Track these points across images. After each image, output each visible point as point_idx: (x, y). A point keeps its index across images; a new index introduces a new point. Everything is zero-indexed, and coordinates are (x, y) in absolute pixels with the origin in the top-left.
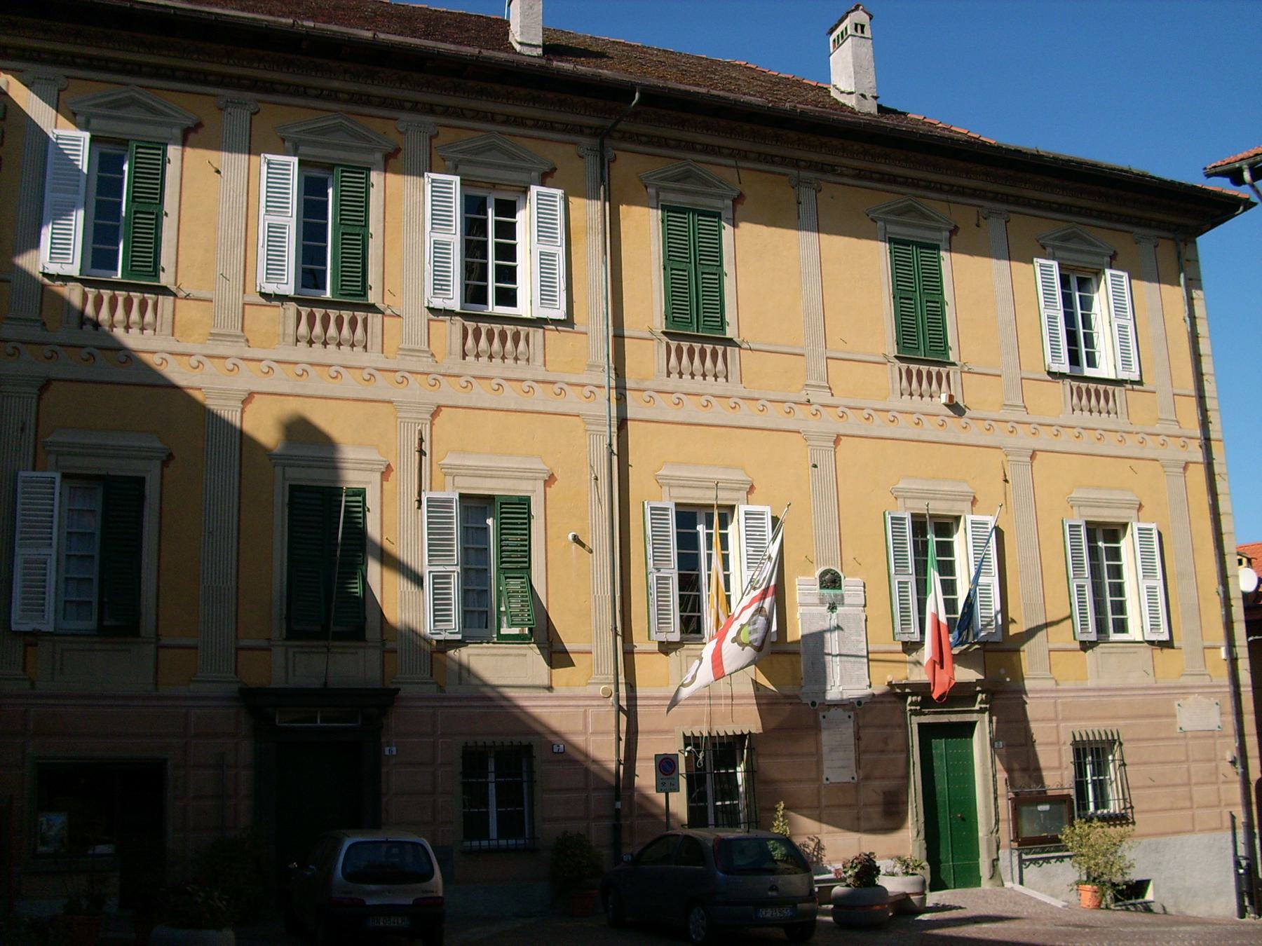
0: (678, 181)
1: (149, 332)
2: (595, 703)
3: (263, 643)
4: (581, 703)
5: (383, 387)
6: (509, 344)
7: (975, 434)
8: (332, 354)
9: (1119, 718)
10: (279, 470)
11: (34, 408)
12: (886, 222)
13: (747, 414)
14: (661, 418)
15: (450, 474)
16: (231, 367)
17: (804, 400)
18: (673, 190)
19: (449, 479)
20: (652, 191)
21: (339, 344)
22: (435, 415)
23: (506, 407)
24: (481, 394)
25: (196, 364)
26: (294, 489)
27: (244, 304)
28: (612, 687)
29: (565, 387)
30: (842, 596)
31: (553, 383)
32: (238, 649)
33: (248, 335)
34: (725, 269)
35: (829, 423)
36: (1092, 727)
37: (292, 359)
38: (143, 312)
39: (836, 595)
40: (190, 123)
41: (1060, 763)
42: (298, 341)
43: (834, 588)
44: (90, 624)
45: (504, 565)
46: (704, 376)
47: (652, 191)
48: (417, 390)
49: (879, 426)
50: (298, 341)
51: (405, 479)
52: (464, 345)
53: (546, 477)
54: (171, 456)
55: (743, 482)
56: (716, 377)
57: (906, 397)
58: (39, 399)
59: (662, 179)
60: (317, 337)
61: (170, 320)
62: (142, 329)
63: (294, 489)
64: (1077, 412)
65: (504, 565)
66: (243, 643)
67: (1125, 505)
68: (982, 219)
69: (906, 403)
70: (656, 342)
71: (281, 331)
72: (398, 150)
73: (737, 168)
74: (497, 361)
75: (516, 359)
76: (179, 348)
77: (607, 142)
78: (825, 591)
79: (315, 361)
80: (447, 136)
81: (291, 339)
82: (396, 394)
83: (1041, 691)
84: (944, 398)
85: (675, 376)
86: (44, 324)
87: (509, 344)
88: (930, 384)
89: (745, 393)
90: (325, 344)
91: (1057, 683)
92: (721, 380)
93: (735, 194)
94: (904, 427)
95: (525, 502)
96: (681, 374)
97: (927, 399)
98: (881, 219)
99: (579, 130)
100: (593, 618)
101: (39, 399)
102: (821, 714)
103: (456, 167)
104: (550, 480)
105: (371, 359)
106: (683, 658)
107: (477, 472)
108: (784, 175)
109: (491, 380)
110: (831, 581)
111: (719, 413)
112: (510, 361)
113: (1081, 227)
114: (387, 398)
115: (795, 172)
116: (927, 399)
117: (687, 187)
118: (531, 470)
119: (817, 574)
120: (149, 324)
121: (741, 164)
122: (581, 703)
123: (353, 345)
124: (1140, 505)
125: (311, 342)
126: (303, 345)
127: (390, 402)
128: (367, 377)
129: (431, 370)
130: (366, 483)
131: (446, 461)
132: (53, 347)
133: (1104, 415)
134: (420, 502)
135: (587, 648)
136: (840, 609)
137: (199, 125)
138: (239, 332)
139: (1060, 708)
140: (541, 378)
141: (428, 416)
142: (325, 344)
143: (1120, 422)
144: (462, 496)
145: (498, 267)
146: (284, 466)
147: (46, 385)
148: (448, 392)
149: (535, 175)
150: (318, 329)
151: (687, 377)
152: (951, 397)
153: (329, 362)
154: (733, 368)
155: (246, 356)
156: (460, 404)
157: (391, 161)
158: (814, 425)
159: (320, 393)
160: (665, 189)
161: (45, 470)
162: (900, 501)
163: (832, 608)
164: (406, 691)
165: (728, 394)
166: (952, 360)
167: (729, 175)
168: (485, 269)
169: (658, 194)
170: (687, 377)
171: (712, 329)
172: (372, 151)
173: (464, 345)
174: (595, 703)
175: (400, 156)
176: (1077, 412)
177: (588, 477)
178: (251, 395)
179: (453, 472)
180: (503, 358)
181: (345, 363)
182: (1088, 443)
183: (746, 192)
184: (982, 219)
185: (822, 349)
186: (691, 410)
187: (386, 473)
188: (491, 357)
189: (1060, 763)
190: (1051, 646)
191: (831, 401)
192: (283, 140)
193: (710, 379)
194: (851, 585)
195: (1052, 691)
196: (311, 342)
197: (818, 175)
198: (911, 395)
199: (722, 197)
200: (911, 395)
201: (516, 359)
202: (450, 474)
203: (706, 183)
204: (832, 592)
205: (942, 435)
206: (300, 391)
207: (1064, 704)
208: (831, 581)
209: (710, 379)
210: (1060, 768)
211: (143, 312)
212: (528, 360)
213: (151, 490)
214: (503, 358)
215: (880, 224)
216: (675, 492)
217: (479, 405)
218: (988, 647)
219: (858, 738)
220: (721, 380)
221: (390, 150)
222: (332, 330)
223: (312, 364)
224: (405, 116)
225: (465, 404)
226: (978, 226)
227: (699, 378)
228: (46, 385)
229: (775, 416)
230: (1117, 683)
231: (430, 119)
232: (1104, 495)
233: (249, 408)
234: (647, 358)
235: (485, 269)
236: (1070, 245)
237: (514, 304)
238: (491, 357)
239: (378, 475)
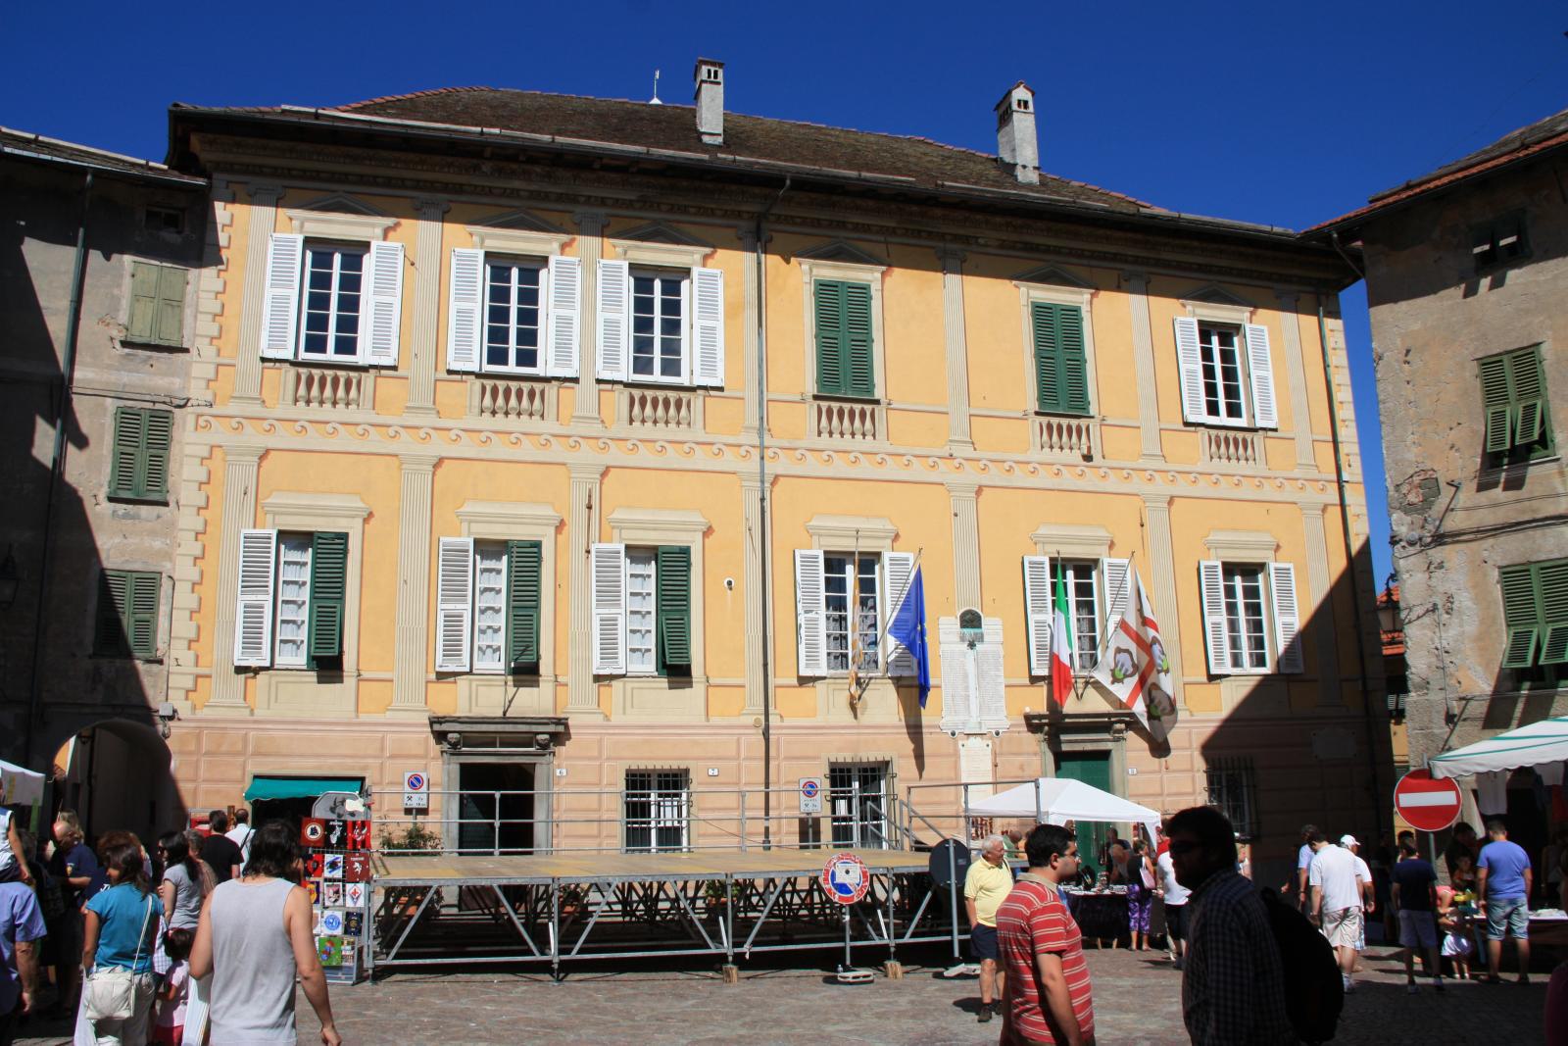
1: (353, 407)
5: (558, 451)
6: (672, 410)
7: (1113, 483)
13: (892, 469)
15: (618, 527)
17: (947, 455)
19: (616, 532)
21: (519, 414)
22: (604, 475)
24: (645, 456)
27: (436, 381)
30: (982, 635)
31: (712, 444)
33: (438, 408)
35: (972, 476)
39: (976, 634)
42: (482, 411)
46: (853, 434)
49: (1020, 478)
50: (482, 411)
52: (631, 411)
53: (704, 528)
54: (371, 515)
56: (864, 435)
57: (1047, 450)
58: (259, 466)
62: (348, 404)
70: (807, 406)
71: (468, 404)
74: (661, 425)
75: (678, 423)
78: (966, 630)
81: (477, 410)
82: (569, 457)
85: (825, 435)
86: (264, 402)
87: (672, 410)
89: (891, 449)
90: (507, 413)
92: (869, 438)
94: (1045, 479)
95: (685, 552)
96: (831, 434)
101: (259, 466)
102: (960, 743)
103: (625, 253)
104: (708, 532)
105: (549, 426)
109: (656, 442)
110: (971, 620)
111: (866, 468)
123: (531, 415)
125: (494, 413)
126: (487, 415)
127: (564, 464)
133: (1243, 462)
134: (588, 552)
136: (979, 646)
138: (431, 405)
141: (598, 476)
142: (507, 413)
146: (470, 522)
148: (616, 455)
150: (500, 400)
151: (836, 436)
155: (437, 426)
163: (972, 645)
165: (875, 450)
166: (1092, 413)
170: (836, 436)
171: (861, 391)
173: (631, 411)
179: (620, 525)
182: (1225, 489)
186: (840, 467)
187: (560, 527)
188: (655, 422)
193: (859, 437)
194: (990, 625)
196: (494, 413)
200: (1051, 447)
201: (678, 423)
202: (618, 527)
205: (1081, 484)
208: (971, 620)
209: (859, 437)
212: (689, 424)
213: (354, 544)
214: (667, 423)
220: (869, 438)
222: (513, 401)
224: (579, 209)
227: (848, 437)
229: (919, 471)
231: (602, 211)
232: (1243, 537)
233: (439, 472)
238: (655, 422)
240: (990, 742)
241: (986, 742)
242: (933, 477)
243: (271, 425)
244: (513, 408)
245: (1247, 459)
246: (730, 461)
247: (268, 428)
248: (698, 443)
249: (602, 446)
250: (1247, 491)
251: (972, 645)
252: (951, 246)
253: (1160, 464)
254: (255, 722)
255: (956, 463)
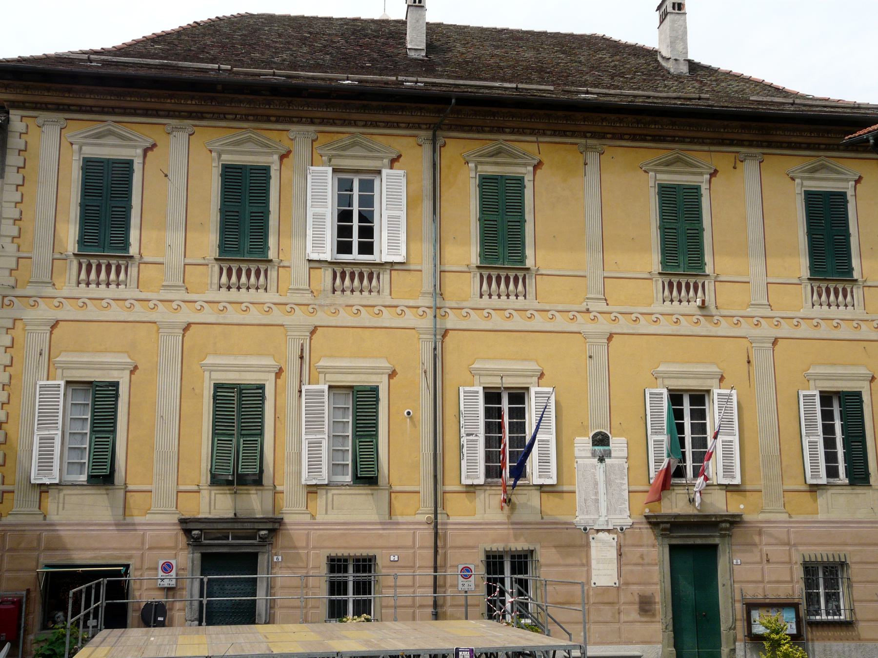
0: (492, 156)
1: (122, 287)
2: (422, 527)
3: (195, 488)
4: (411, 527)
5: (277, 316)
6: (366, 282)
7: (724, 328)
8: (243, 295)
9: (847, 544)
10: (207, 374)
11: (48, 339)
12: (656, 172)
13: (539, 322)
14: (475, 328)
15: (322, 372)
16: (176, 307)
17: (584, 309)
18: (488, 163)
19: (322, 376)
20: (472, 165)
21: (248, 288)
22: (313, 332)
23: (362, 325)
24: (345, 318)
25: (129, 306)
26: (218, 387)
27: (185, 265)
28: (432, 516)
29: (448, 310)
30: (610, 451)
31: (397, 307)
32: (178, 492)
33: (188, 286)
34: (527, 217)
35: (604, 326)
36: (822, 552)
37: (217, 299)
38: (118, 274)
39: (605, 451)
40: (148, 145)
41: (792, 577)
42: (220, 287)
43: (604, 445)
44: (84, 478)
45: (243, 432)
46: (508, 296)
47: (472, 165)
48: (300, 317)
49: (644, 326)
50: (220, 287)
51: (291, 378)
52: (334, 284)
53: (390, 372)
54: (136, 368)
55: (534, 371)
56: (517, 296)
57: (668, 303)
58: (51, 333)
59: (480, 156)
60: (233, 284)
61: (136, 278)
62: (118, 285)
63: (218, 387)
64: (817, 307)
65: (243, 432)
66: (182, 488)
67: (709, 376)
68: (738, 161)
69: (668, 307)
70: (472, 275)
71: (209, 282)
72: (289, 152)
73: (538, 142)
74: (357, 293)
75: (370, 291)
76: (143, 296)
77: (438, 133)
78: (596, 448)
79: (232, 300)
80: (323, 139)
81: (216, 287)
82: (286, 320)
83: (354, 524)
84: (699, 302)
85: (486, 297)
86: (54, 285)
87: (366, 282)
88: (688, 292)
89: (539, 307)
90: (239, 288)
91: (790, 516)
92: (521, 298)
93: (536, 162)
94: (664, 326)
95: (375, 390)
96: (490, 296)
97: (685, 303)
98: (652, 170)
99: (418, 126)
100: (421, 468)
101: (51, 333)
102: (591, 537)
103: (330, 160)
104: (392, 375)
105: (271, 297)
106: (487, 495)
107: (226, 368)
108: (576, 144)
109: (352, 308)
110: (601, 440)
111: (518, 322)
112: (366, 293)
113: (831, 160)
114: (280, 322)
115: (583, 141)
116: (685, 303)
117: (499, 160)
118: (379, 368)
119: (591, 435)
120: (122, 281)
121: (541, 139)
122: (411, 527)
123: (257, 288)
124: (722, 376)
125: (229, 288)
126: (224, 290)
127: (282, 325)
128: (267, 309)
129: (311, 302)
130: (267, 380)
131: (320, 364)
132: (108, 301)
133: (842, 308)
134: (300, 391)
135: (416, 489)
136: (607, 460)
137: (154, 145)
138: (181, 283)
139: (792, 536)
140: (387, 304)
141: (308, 334)
142: (239, 288)
143: (858, 312)
144: (330, 387)
145: (360, 228)
146: (211, 371)
147: (55, 325)
148: (321, 318)
149: (386, 161)
150: (234, 278)
151: (495, 297)
152: (703, 302)
153: (262, 301)
154: (531, 289)
155: (186, 299)
156: (330, 324)
157: (285, 160)
158: (589, 328)
159: (235, 321)
160: (482, 163)
161: (55, 379)
162: (660, 381)
163: (601, 460)
164: (287, 519)
165: (526, 307)
166: (707, 272)
167: (532, 148)
168: (354, 228)
169: (476, 167)
170: (495, 297)
171: (515, 261)
172: (272, 154)
173: (334, 284)
174: (422, 527)
175: (291, 156)
176: (817, 307)
177: (420, 371)
178: (57, 322)
179: (325, 371)
180: (361, 291)
181: (252, 301)
182: (825, 331)
183: (544, 160)
184: (738, 161)
185: (600, 271)
186: (497, 321)
187: (279, 373)
188: (352, 291)
189: (792, 577)
190: (786, 487)
191: (605, 308)
192: (211, 151)
193: (513, 298)
194: (618, 444)
195: (786, 522)
196: (229, 288)
197: (600, 142)
198: (672, 301)
199: (525, 165)
200: (672, 301)
201: (370, 291)
202: (322, 372)
203: (515, 156)
204: (602, 448)
205: (697, 330)
206: (221, 321)
207: (796, 532)
208: (601, 440)
209: (513, 298)
210: (792, 581)
211: (118, 274)
212: (379, 292)
213: (123, 390)
214: (361, 291)
215: (652, 174)
216: (483, 379)
217: (344, 325)
218: (544, 489)
219: (620, 555)
220: (521, 298)
221: (284, 152)
222: (244, 279)
223: (230, 303)
224: (295, 128)
225: (334, 324)
226: (735, 168)
227: (504, 298)
228: (55, 325)
229: (561, 323)
230: (846, 517)
231: (312, 128)
232: (840, 370)
233: (188, 333)
234: (465, 287)
235: (354, 228)
236: (817, 175)
237: (371, 252)
238: (352, 291)
239: (273, 375)
240: (615, 536)
241: (612, 536)
242: (573, 327)
243: (84, 303)
244: (243, 284)
245: (846, 306)
246: (410, 319)
247: (57, 304)
248: (385, 306)
249: (312, 311)
250: (846, 332)
251: (601, 460)
252: (591, 142)
253: (767, 312)
254: (47, 525)
255: (591, 316)
